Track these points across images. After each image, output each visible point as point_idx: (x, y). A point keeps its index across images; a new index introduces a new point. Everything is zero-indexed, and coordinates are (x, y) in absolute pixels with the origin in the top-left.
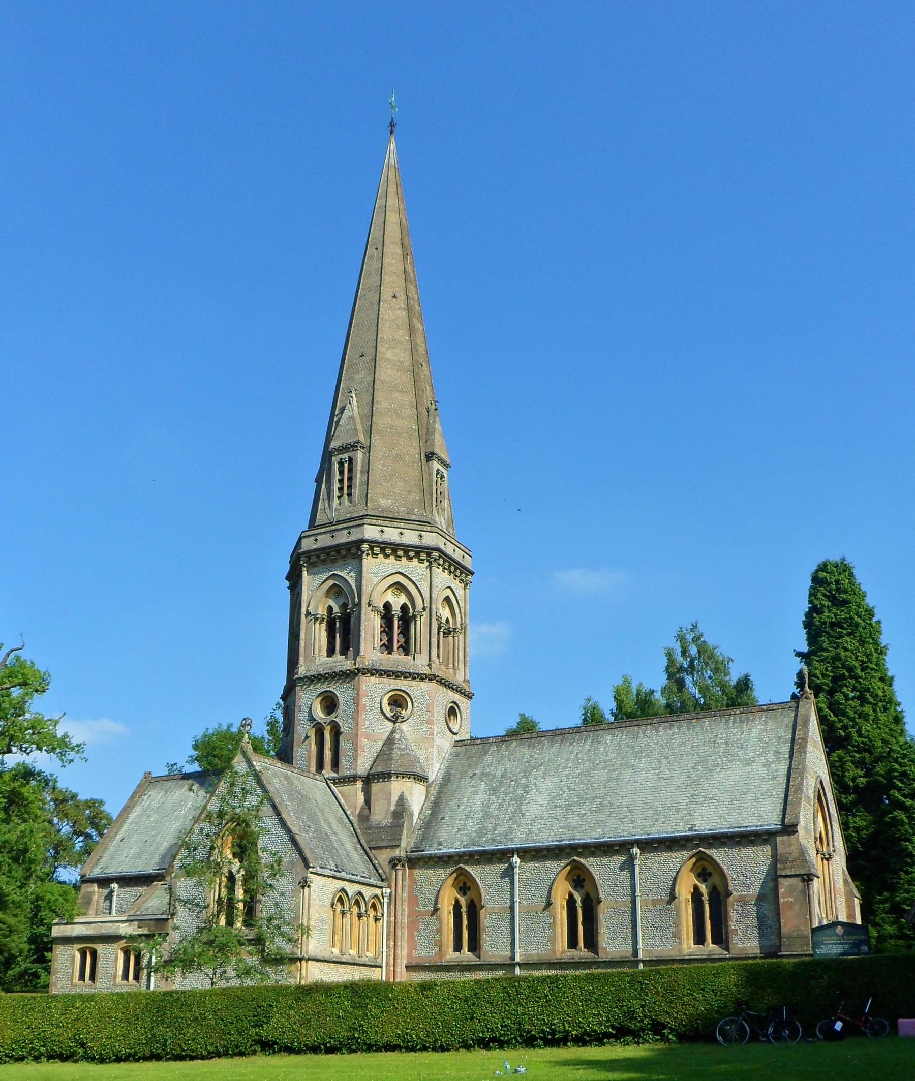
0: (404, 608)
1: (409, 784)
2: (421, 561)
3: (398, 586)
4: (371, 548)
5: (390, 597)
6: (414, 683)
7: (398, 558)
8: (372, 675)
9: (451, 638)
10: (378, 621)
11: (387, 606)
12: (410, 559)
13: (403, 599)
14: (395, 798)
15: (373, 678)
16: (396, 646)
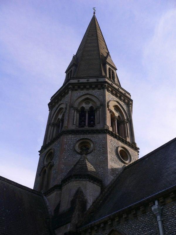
0: (91, 108)
1: (84, 182)
2: (99, 89)
3: (87, 100)
4: (74, 87)
5: (84, 105)
6: (95, 135)
7: (88, 89)
8: (70, 134)
9: (122, 125)
10: (77, 116)
11: (83, 108)
12: (94, 89)
13: (90, 105)
14: (74, 192)
15: (70, 136)
16: (87, 124)
